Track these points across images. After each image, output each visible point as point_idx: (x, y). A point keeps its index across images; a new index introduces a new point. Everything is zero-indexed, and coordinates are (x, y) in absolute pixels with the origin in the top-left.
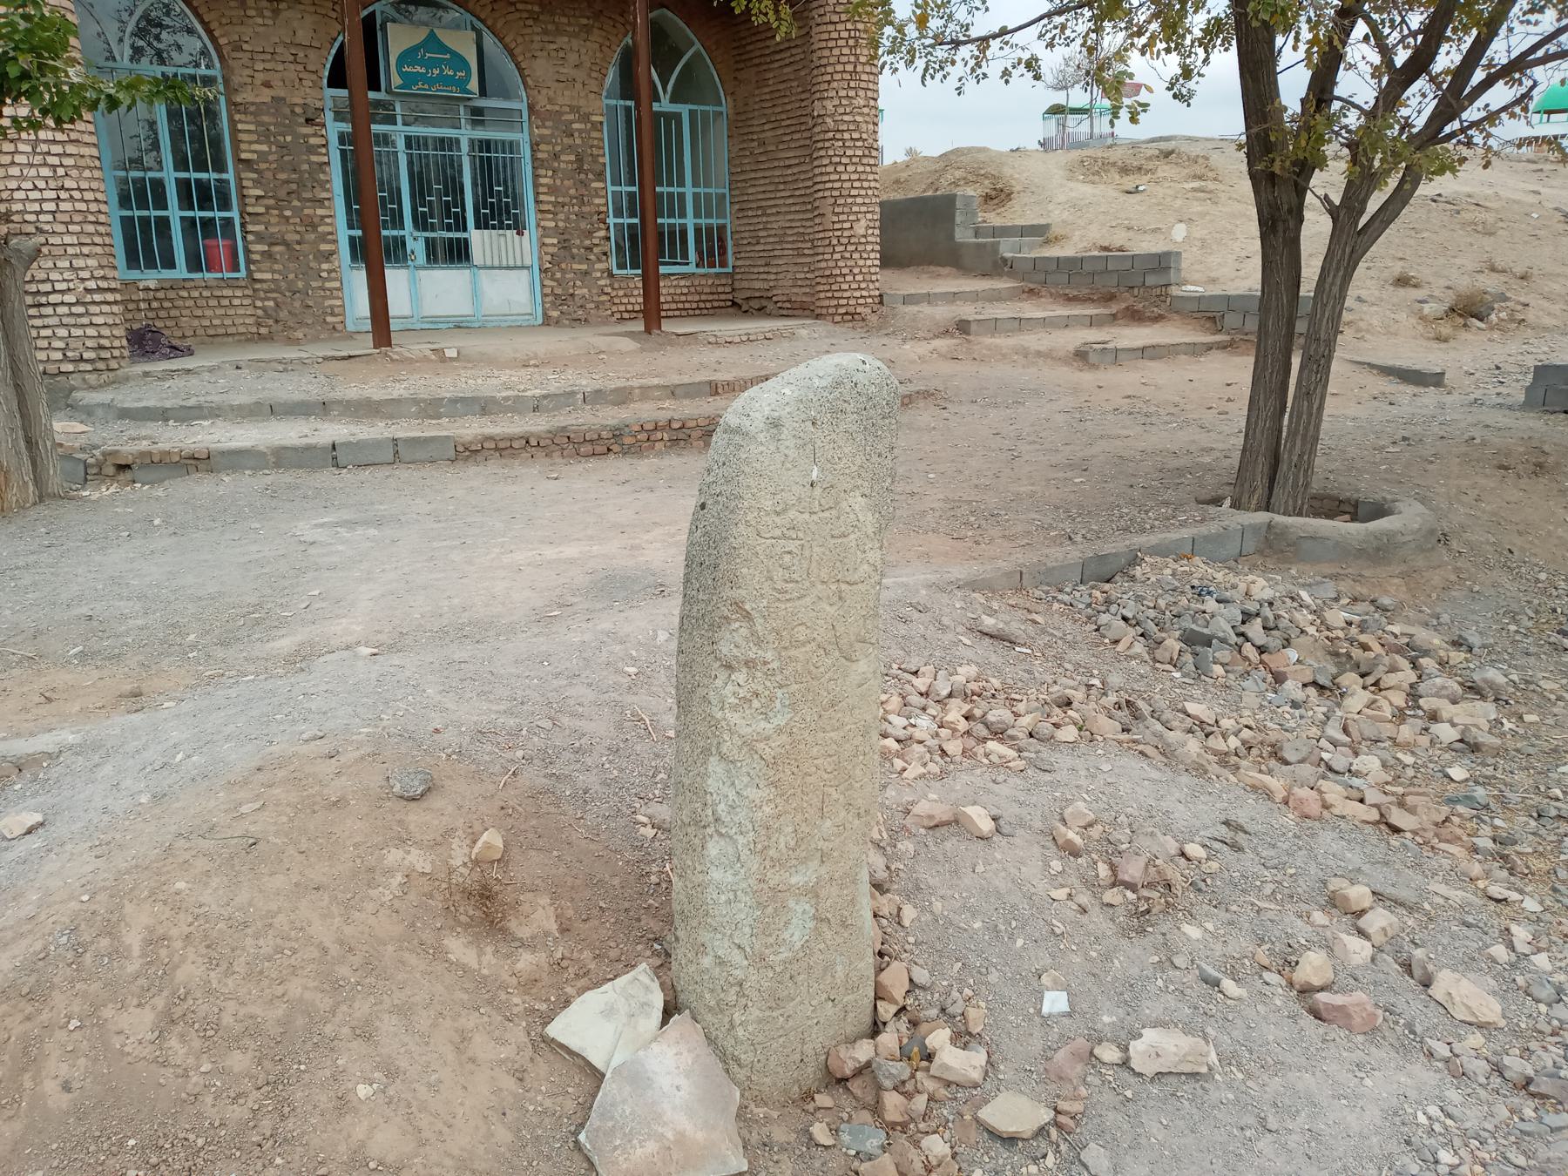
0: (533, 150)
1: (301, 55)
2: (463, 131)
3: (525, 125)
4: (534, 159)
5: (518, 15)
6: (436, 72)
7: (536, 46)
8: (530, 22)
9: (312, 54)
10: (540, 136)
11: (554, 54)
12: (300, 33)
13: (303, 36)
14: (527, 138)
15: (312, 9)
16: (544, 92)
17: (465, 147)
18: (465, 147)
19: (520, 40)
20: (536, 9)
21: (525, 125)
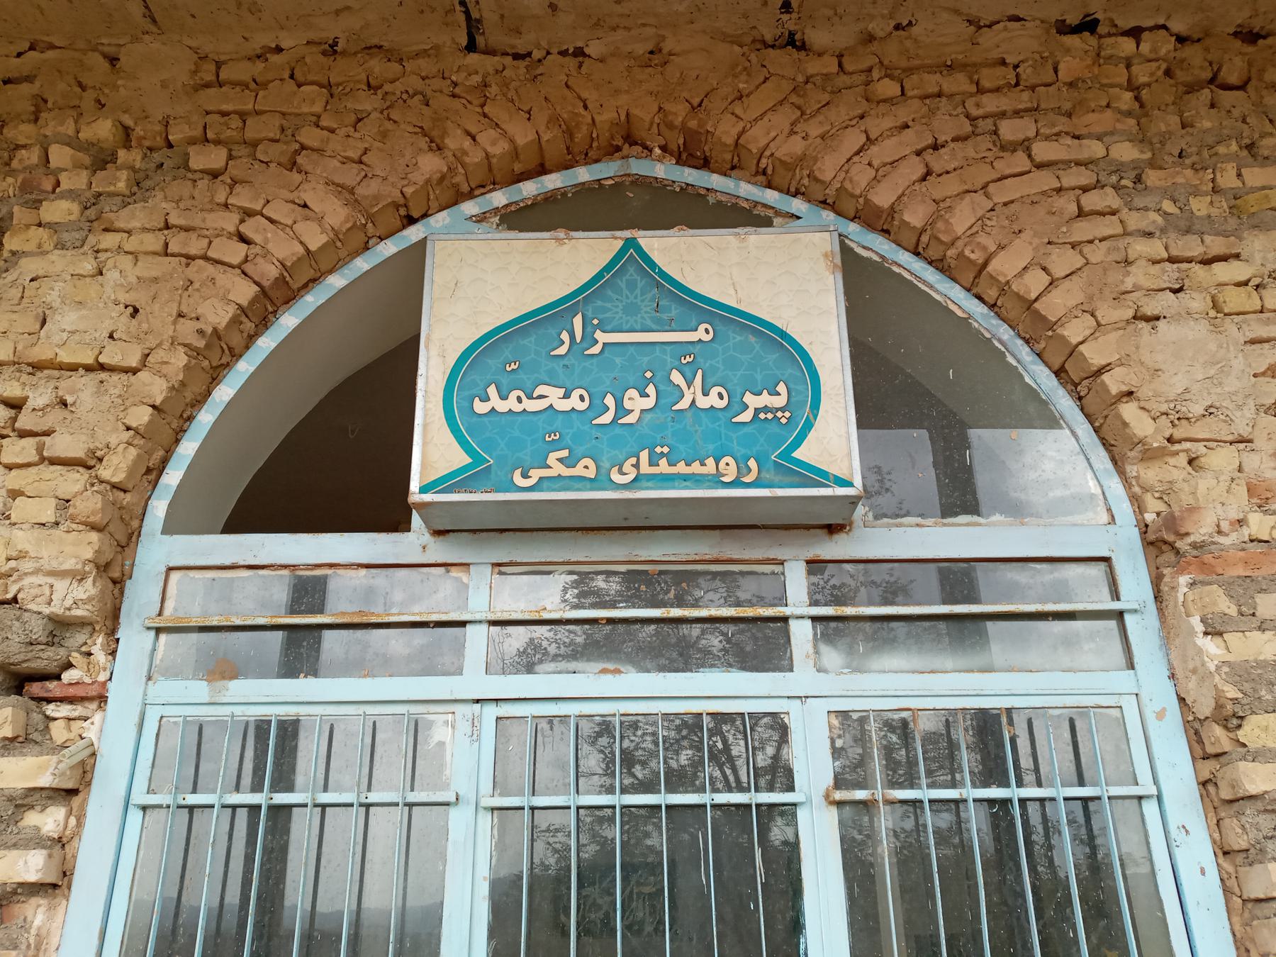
0: (1201, 753)
1: (39, 396)
2: (802, 677)
3: (1142, 629)
4: (1220, 800)
5: (1046, 180)
6: (636, 403)
7: (1140, 275)
8: (1107, 199)
9: (83, 389)
10: (1240, 672)
11: (1235, 299)
12: (66, 319)
13: (75, 328)
14: (1161, 695)
15: (153, 242)
16: (1222, 459)
17: (812, 763)
18: (812, 763)
19: (1062, 261)
20: (1126, 152)
21: (1142, 629)
